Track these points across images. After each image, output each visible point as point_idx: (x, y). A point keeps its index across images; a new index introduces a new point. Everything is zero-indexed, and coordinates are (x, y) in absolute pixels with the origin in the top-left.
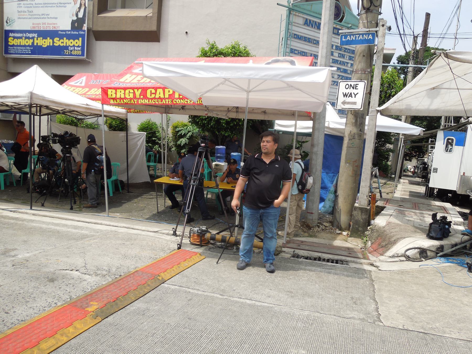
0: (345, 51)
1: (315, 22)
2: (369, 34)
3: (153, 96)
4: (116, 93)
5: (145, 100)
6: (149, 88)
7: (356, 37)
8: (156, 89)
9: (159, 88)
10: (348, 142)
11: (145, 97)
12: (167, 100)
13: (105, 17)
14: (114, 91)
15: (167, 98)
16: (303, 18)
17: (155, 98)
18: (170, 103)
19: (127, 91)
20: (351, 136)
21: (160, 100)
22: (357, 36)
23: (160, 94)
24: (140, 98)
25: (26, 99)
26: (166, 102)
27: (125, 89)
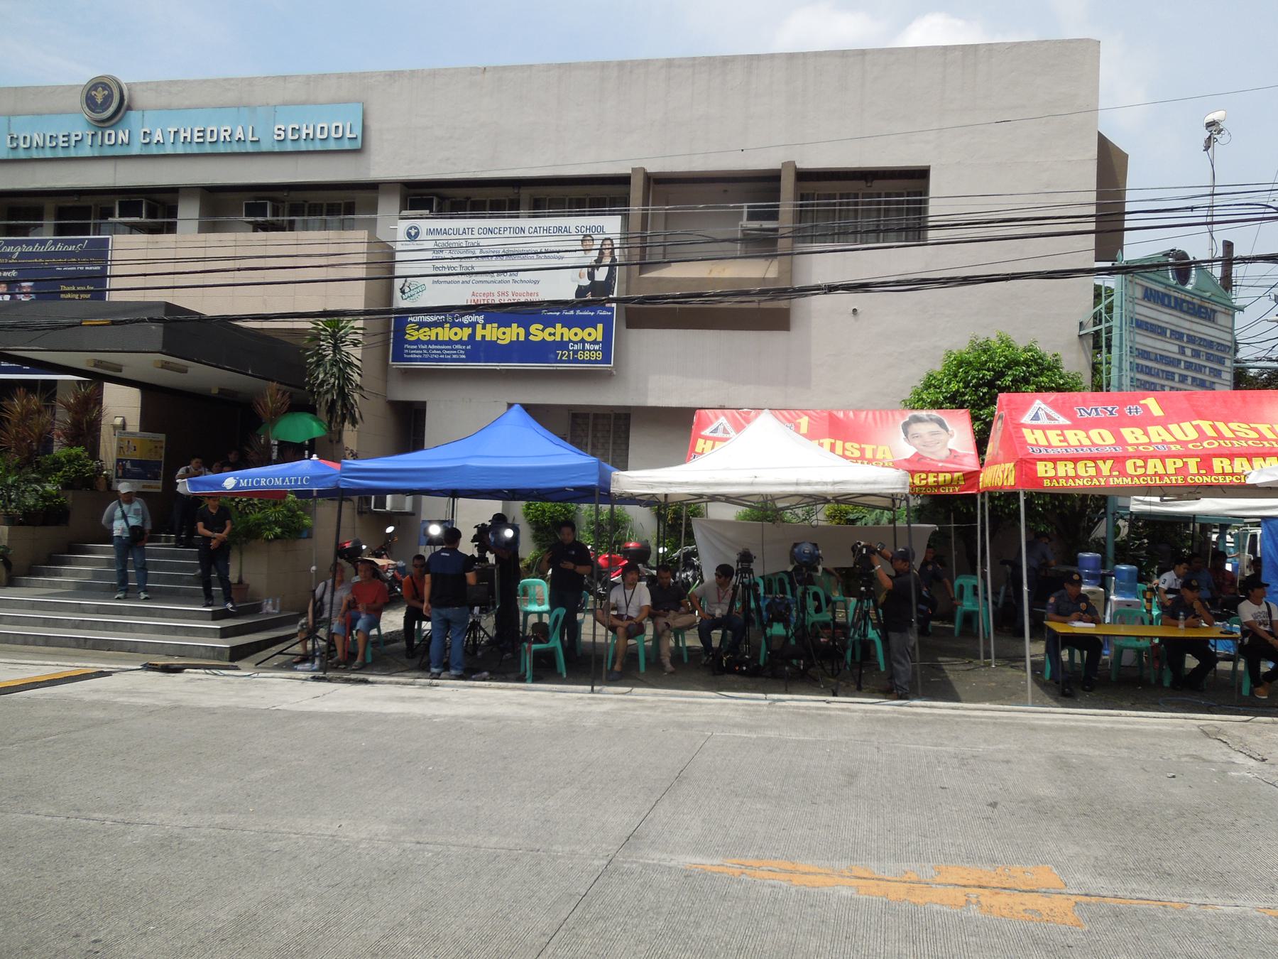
0: (1199, 345)
1: (1158, 292)
3: (1141, 471)
4: (1055, 468)
5: (1125, 479)
6: (1130, 458)
11: (1123, 473)
12: (1173, 478)
13: (659, 280)
14: (1050, 465)
15: (1172, 475)
17: (1145, 475)
18: (1180, 482)
19: (1080, 465)
21: (1157, 478)
24: (1111, 476)
25: (897, 486)
26: (1171, 480)
27: (1075, 460)
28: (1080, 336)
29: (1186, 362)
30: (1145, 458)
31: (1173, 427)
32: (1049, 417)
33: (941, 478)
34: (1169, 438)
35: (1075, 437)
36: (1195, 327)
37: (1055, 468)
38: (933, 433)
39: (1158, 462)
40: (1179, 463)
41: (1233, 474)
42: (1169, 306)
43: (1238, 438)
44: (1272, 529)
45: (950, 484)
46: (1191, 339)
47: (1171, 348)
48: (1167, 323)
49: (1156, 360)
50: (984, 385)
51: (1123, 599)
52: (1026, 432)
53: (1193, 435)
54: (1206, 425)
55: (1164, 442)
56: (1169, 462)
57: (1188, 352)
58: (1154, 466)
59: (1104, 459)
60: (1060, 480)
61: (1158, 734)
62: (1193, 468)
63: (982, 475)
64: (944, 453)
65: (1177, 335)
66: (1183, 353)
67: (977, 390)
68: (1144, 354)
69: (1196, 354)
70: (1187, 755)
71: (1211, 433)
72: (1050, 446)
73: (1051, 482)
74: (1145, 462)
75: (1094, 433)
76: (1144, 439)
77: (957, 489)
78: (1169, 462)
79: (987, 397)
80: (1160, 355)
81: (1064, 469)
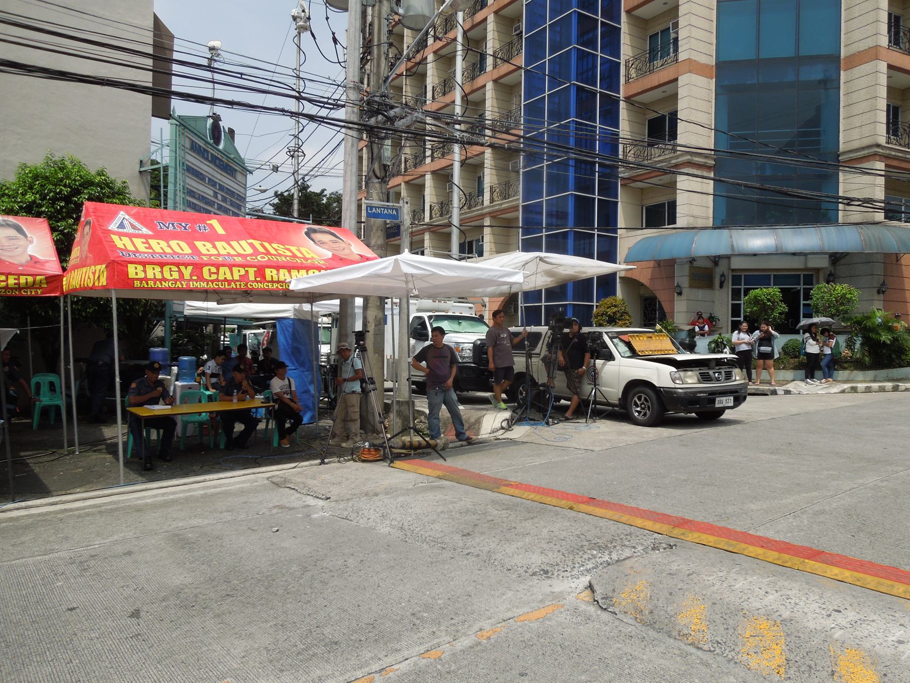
0: (226, 193)
2: (393, 209)
3: (214, 277)
4: (145, 271)
5: (201, 283)
6: (206, 265)
7: (381, 210)
8: (218, 266)
9: (223, 265)
10: (374, 329)
11: (201, 278)
12: (238, 283)
14: (140, 268)
15: (237, 281)
16: (190, 139)
17: (217, 280)
18: (242, 287)
19: (166, 268)
20: (377, 321)
21: (226, 283)
22: (382, 209)
23: (225, 274)
26: (236, 285)
27: (162, 265)
28: (140, 172)
29: (218, 204)
30: (218, 266)
31: (234, 243)
32: (132, 225)
33: (23, 280)
34: (232, 252)
35: (158, 246)
36: (224, 179)
37: (145, 271)
38: (10, 238)
39: (227, 269)
40: (243, 272)
41: (278, 282)
42: (207, 159)
43: (280, 255)
44: (283, 326)
45: (33, 286)
46: (222, 188)
47: (208, 192)
48: (206, 172)
49: (198, 199)
50: (61, 199)
51: (185, 383)
52: (115, 238)
53: (249, 251)
54: (257, 243)
55: (229, 255)
56: (235, 270)
57: (220, 197)
58: (224, 273)
59: (186, 265)
60: (149, 282)
61: (242, 492)
62: (252, 277)
63: (64, 279)
64: (24, 259)
65: (212, 183)
66: (216, 198)
67: (53, 204)
68: (191, 193)
69: (224, 199)
70: (275, 507)
71: (261, 250)
72: (137, 251)
73: (141, 284)
74: (218, 270)
75: (173, 243)
76: (214, 251)
77: (39, 291)
78: (235, 270)
79: (64, 210)
80: (202, 196)
81: (152, 272)
